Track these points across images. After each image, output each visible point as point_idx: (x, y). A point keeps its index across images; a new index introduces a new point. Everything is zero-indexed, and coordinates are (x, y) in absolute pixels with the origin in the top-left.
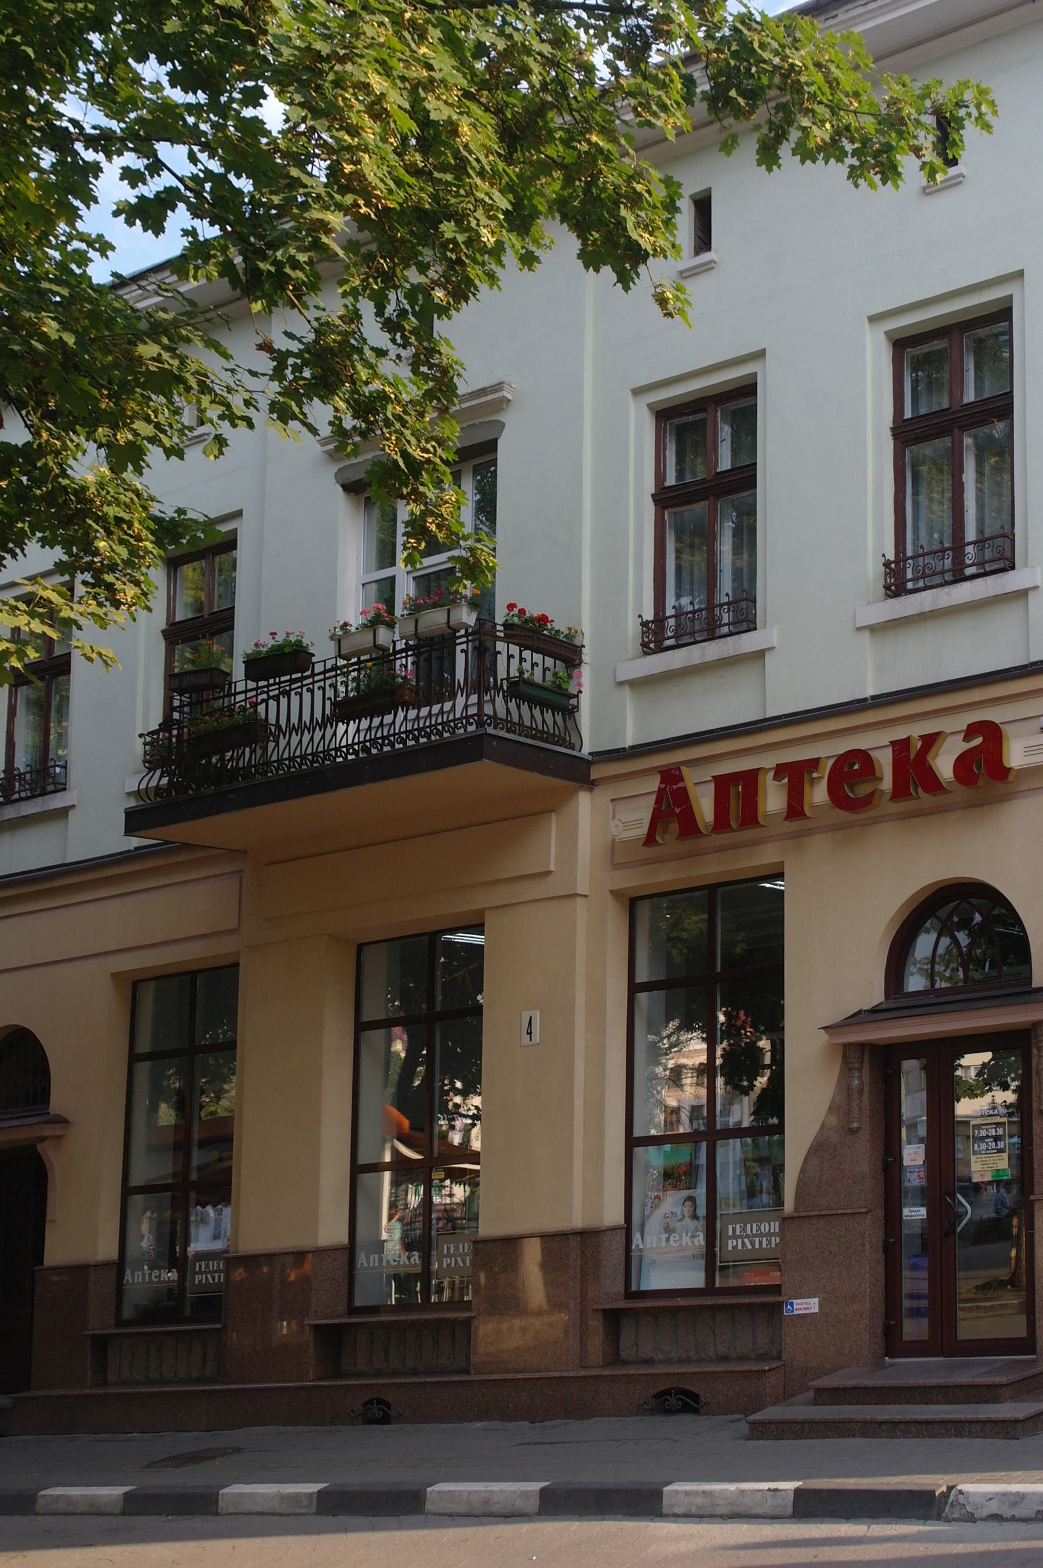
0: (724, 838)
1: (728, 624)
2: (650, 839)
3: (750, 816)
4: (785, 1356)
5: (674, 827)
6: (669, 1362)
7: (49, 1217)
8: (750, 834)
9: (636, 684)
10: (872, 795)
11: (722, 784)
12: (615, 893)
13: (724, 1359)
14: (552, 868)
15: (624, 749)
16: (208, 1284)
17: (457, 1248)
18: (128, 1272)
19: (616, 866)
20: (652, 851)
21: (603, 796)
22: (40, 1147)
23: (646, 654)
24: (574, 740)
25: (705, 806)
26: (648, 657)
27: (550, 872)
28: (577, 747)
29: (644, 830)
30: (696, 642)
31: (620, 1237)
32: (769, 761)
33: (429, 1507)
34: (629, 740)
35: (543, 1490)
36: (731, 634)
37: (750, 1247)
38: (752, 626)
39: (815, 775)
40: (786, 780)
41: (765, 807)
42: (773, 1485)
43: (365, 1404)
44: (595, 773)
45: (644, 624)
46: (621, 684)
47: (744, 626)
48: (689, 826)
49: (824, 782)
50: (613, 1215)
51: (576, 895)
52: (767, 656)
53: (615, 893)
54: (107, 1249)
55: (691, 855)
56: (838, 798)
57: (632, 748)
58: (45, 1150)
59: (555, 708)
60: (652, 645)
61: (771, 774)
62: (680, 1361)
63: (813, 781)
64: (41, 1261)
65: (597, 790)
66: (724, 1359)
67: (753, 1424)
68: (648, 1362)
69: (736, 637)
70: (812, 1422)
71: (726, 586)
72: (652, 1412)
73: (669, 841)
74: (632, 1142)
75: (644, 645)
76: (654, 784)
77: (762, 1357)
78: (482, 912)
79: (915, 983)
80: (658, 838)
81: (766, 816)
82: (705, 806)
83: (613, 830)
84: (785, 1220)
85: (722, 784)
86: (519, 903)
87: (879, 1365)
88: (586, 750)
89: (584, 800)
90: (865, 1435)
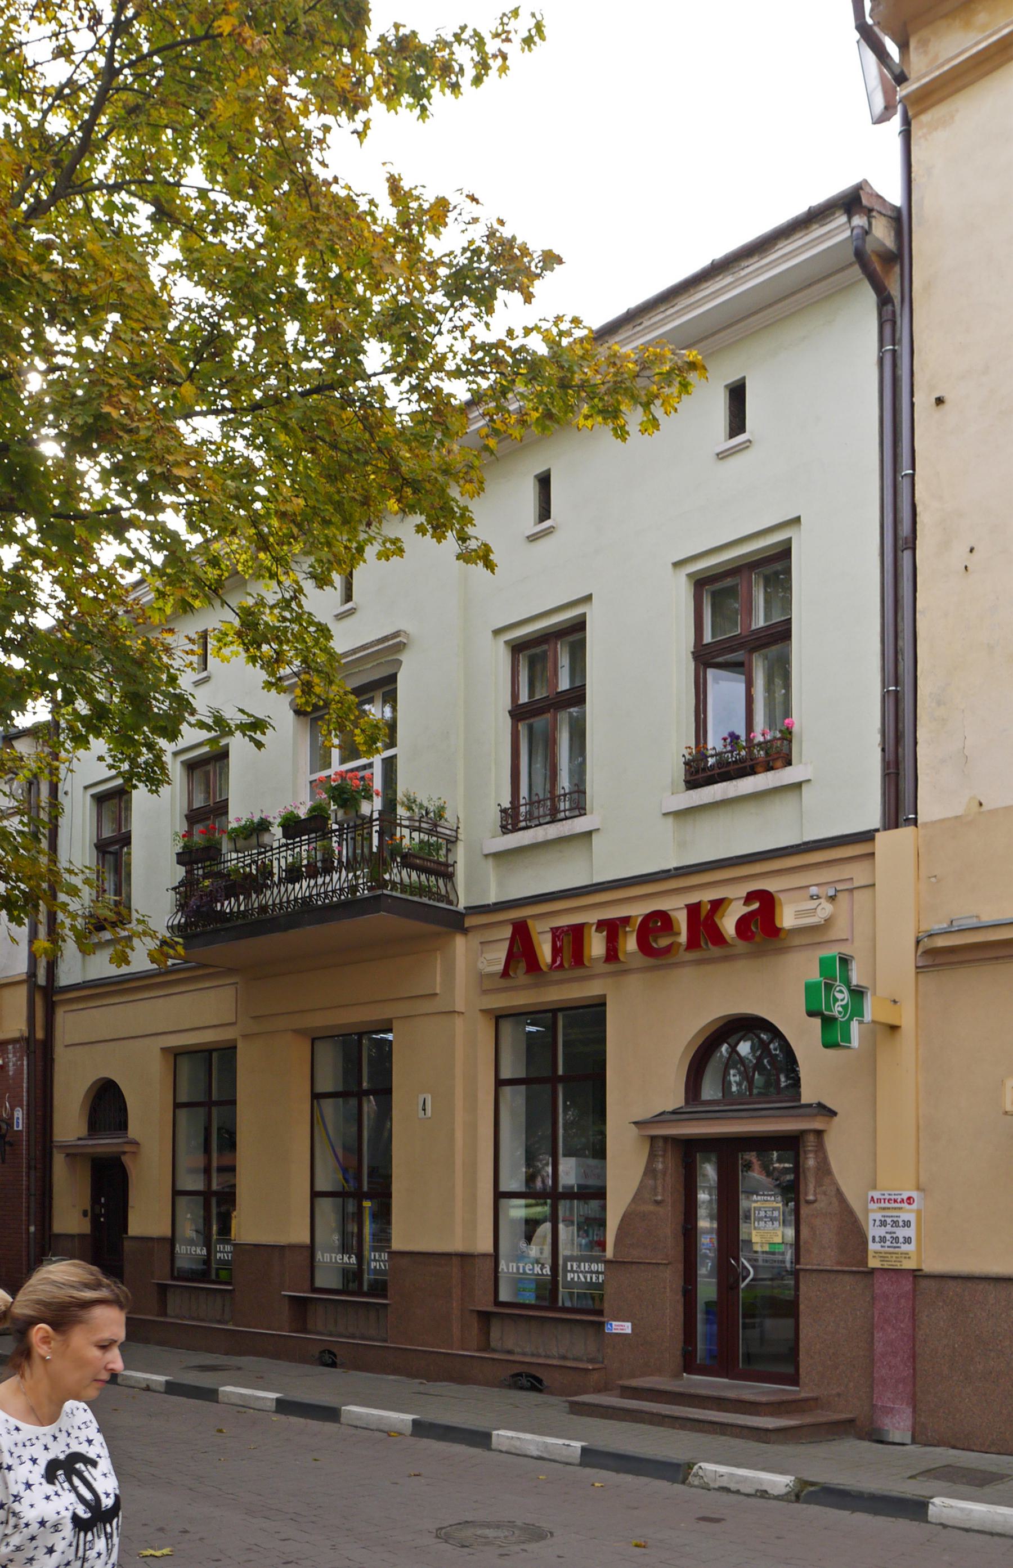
0: (557, 975)
1: (565, 811)
2: (505, 973)
3: (578, 957)
4: (606, 1362)
5: (522, 966)
6: (524, 1354)
7: (130, 1204)
8: (579, 972)
9: (498, 856)
10: (671, 945)
11: (556, 933)
12: (484, 1011)
13: (564, 1358)
14: (438, 991)
15: (489, 905)
16: (224, 1260)
17: (380, 1256)
18: (177, 1246)
19: (485, 992)
20: (504, 983)
21: (475, 939)
22: (124, 1158)
23: (504, 833)
24: (452, 897)
25: (545, 951)
26: (506, 836)
27: (436, 994)
28: (455, 903)
29: (500, 967)
30: (540, 825)
31: (490, 1264)
32: (592, 917)
33: (343, 1420)
34: (492, 898)
35: (414, 1421)
36: (566, 818)
37: (583, 1279)
38: (583, 812)
39: (628, 929)
40: (605, 933)
41: (590, 951)
42: (567, 1442)
43: (321, 1352)
44: (469, 922)
45: (504, 811)
46: (486, 856)
47: (577, 813)
48: (533, 965)
49: (635, 935)
50: (484, 1245)
51: (455, 1012)
52: (594, 836)
53: (484, 1011)
54: (164, 1229)
55: (536, 986)
56: (644, 946)
57: (495, 904)
58: (126, 1159)
59: (438, 874)
60: (510, 827)
61: (594, 928)
62: (533, 1355)
63: (626, 933)
64: (126, 1232)
65: (470, 935)
66: (564, 1358)
67: (573, 1404)
68: (510, 1352)
69: (569, 821)
70: (614, 1408)
71: (564, 782)
72: (509, 1387)
73: (521, 976)
74: (499, 1195)
75: (502, 827)
76: (507, 932)
77: (591, 1361)
78: (390, 1021)
79: (710, 1091)
80: (511, 973)
81: (591, 959)
82: (545, 951)
83: (480, 966)
84: (607, 1262)
85: (556, 933)
86: (415, 1016)
87: (677, 1376)
88: (461, 906)
89: (460, 942)
90: (651, 1423)
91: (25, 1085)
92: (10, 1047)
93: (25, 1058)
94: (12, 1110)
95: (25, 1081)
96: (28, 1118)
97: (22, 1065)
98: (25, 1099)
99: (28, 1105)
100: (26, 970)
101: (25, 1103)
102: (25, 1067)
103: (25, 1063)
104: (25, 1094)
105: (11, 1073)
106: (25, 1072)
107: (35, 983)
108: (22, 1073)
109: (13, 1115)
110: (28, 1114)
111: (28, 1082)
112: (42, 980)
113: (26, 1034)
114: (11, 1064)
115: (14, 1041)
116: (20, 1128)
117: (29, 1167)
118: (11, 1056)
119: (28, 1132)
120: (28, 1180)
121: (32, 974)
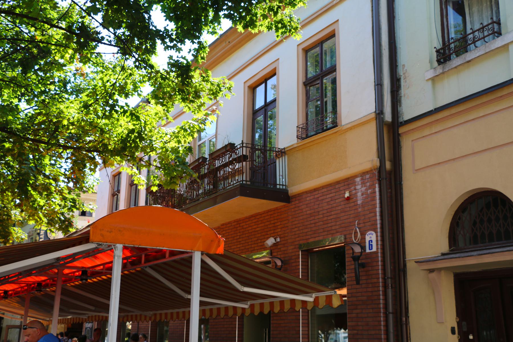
91: (378, 210)
92: (358, 179)
93: (377, 185)
94: (363, 234)
95: (378, 205)
96: (383, 240)
97: (375, 192)
98: (379, 222)
99: (382, 228)
100: (374, 110)
101: (379, 226)
102: (378, 193)
103: (377, 189)
104: (378, 218)
105: (359, 202)
106: (378, 197)
107: (383, 119)
108: (374, 199)
109: (363, 238)
110: (382, 236)
111: (381, 207)
112: (388, 117)
113: (378, 164)
114: (359, 194)
115: (363, 174)
116: (374, 249)
117: (385, 286)
118: (358, 187)
119: (383, 253)
120: (386, 299)
121: (379, 113)
